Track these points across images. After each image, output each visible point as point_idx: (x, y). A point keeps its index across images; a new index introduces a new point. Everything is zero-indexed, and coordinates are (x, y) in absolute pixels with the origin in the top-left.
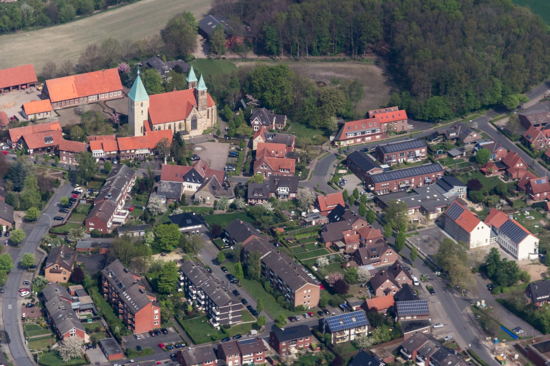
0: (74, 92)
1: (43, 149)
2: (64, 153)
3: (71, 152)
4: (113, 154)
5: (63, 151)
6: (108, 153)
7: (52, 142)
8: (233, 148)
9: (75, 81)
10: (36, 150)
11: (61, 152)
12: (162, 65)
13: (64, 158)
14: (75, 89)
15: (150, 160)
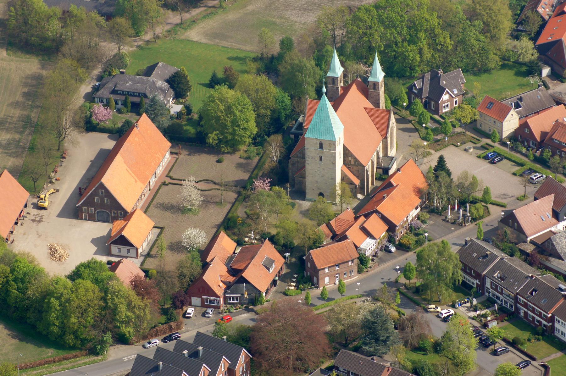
0: (136, 181)
1: (271, 283)
2: (327, 270)
3: (337, 266)
4: (384, 237)
5: (324, 269)
6: (378, 240)
7: (274, 266)
8: (471, 150)
9: (125, 162)
10: (267, 291)
11: (320, 272)
12: (154, 83)
13: (327, 280)
14: (133, 175)
15: (423, 222)
